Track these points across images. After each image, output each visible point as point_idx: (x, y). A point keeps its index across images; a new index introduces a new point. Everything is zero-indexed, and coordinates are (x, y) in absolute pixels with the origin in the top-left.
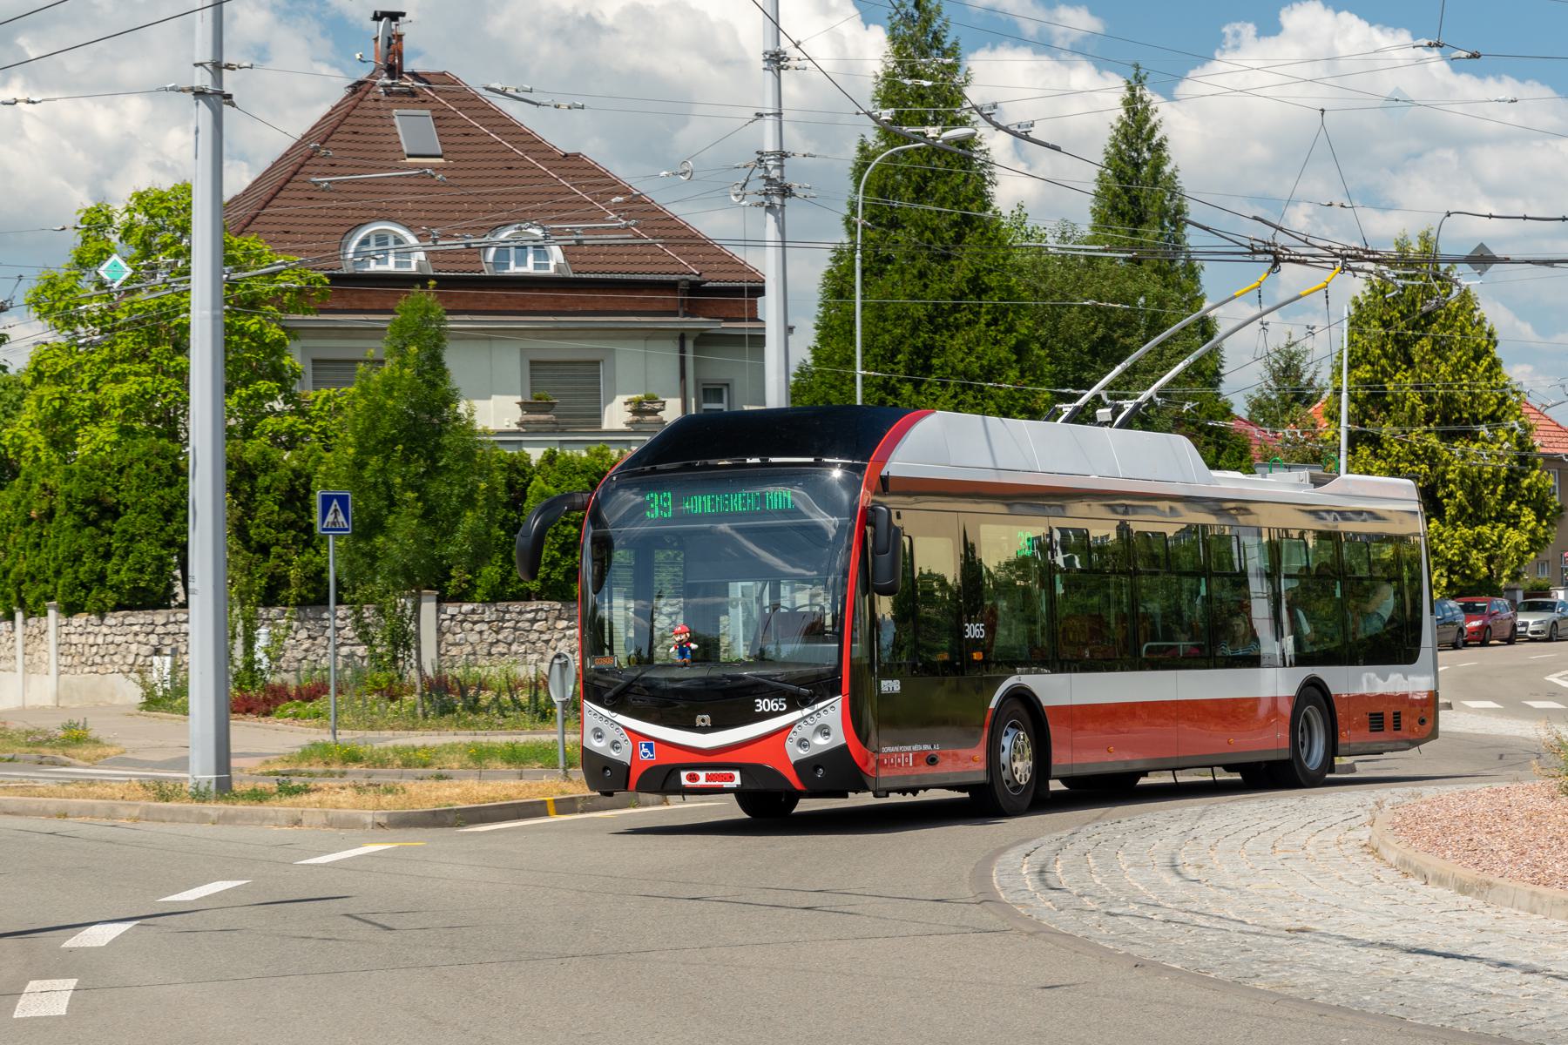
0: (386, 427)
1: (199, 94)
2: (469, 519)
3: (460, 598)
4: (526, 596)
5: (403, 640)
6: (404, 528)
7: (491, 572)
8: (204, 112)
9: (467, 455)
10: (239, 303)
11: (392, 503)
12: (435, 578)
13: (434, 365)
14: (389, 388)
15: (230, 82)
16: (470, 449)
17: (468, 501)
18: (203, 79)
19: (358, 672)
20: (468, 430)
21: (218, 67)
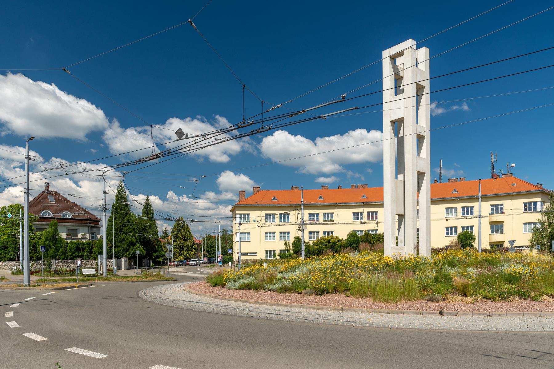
0: (49, 237)
1: (25, 193)
2: (61, 250)
3: (58, 259)
4: (67, 259)
5: (50, 265)
6: (52, 251)
7: (63, 256)
8: (26, 195)
9: (61, 241)
10: (30, 220)
11: (50, 247)
12: (55, 257)
13: (56, 229)
14: (49, 232)
15: (30, 191)
16: (61, 241)
17: (61, 247)
18: (26, 191)
19: (44, 269)
20: (61, 238)
21: (28, 189)
